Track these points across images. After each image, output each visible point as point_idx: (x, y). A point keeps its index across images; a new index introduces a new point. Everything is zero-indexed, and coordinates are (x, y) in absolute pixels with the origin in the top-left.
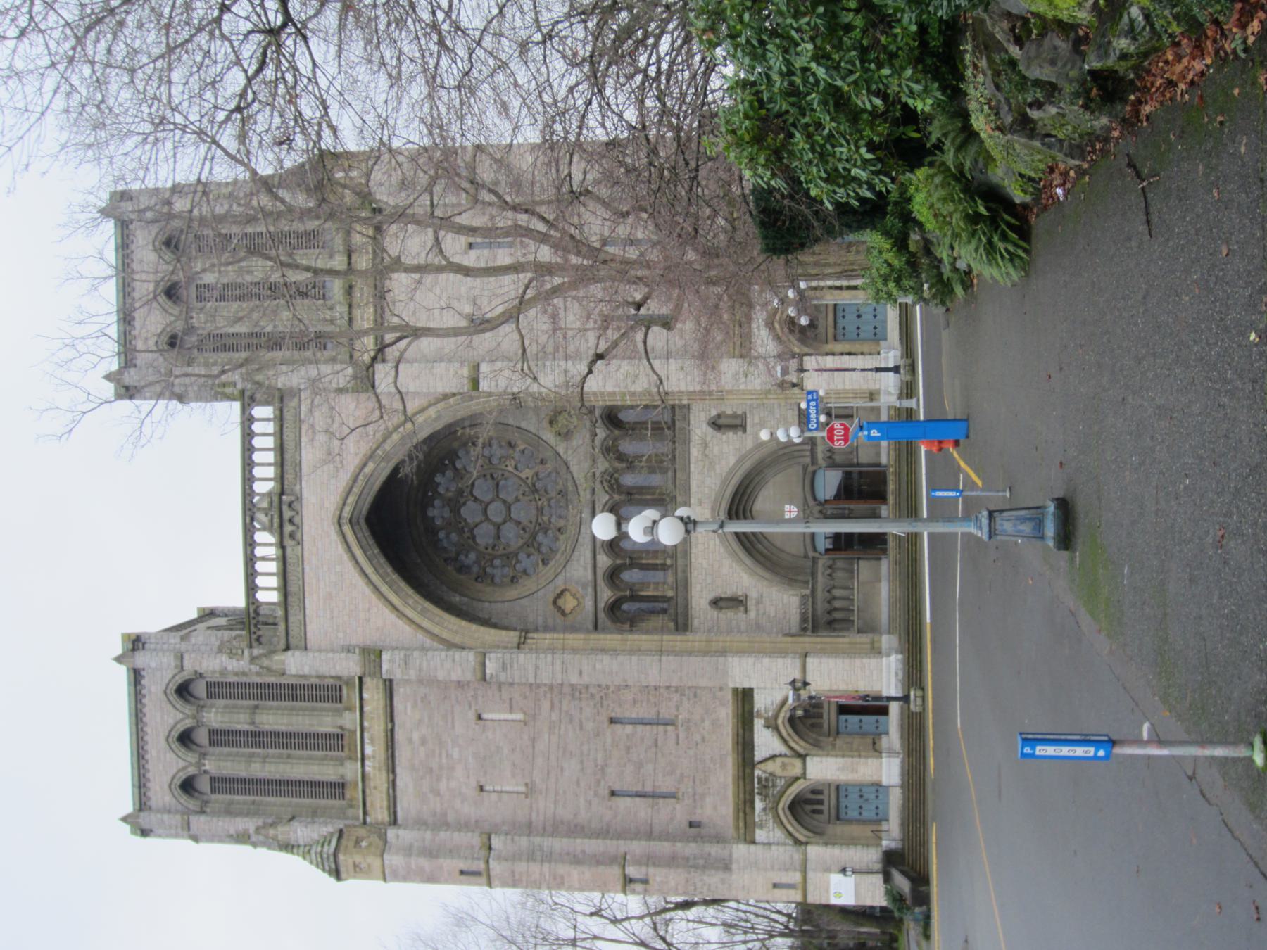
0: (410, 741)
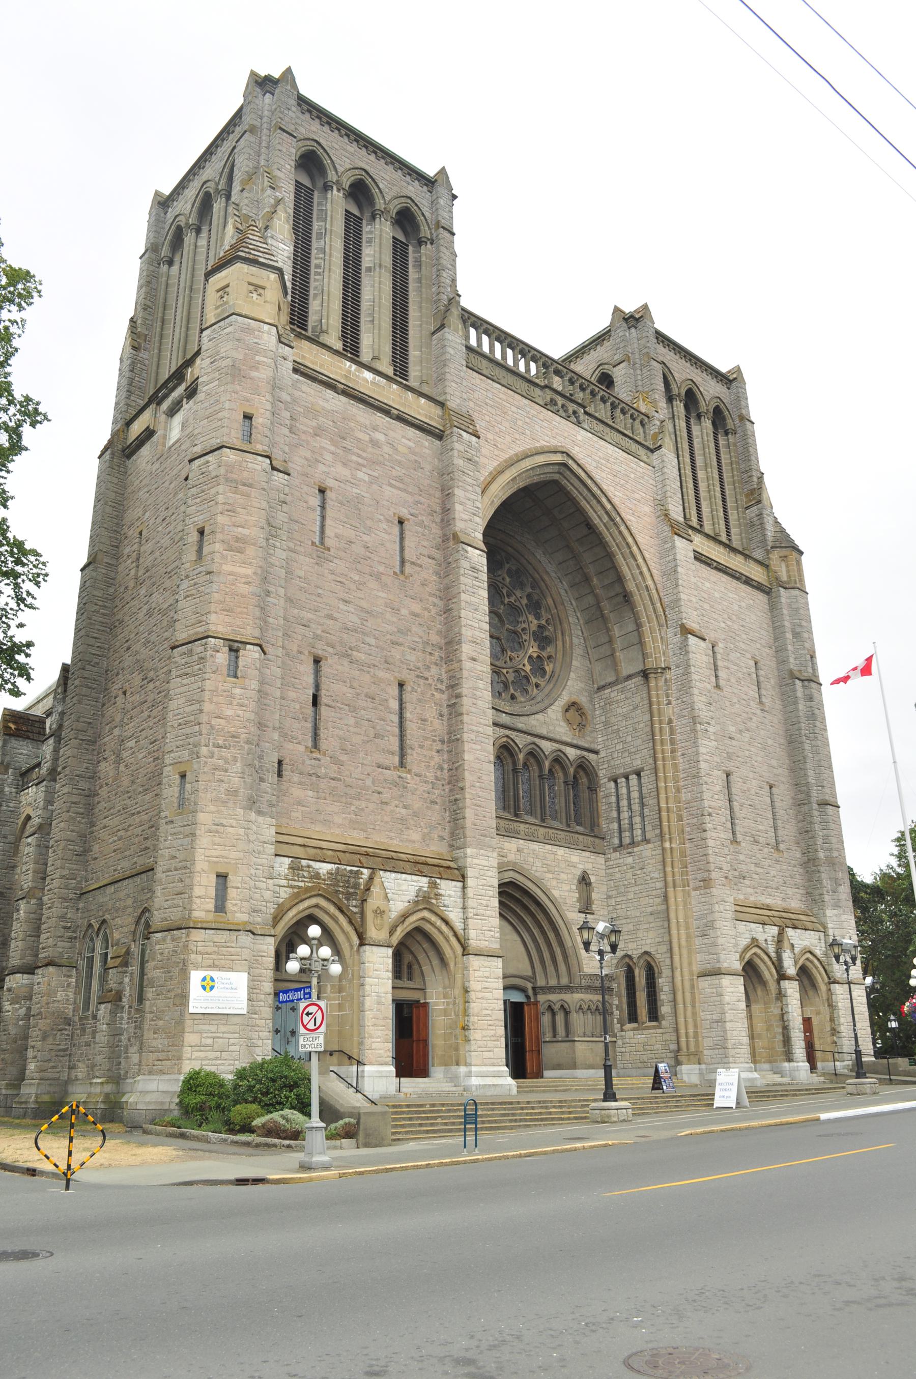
0: (375, 429)
